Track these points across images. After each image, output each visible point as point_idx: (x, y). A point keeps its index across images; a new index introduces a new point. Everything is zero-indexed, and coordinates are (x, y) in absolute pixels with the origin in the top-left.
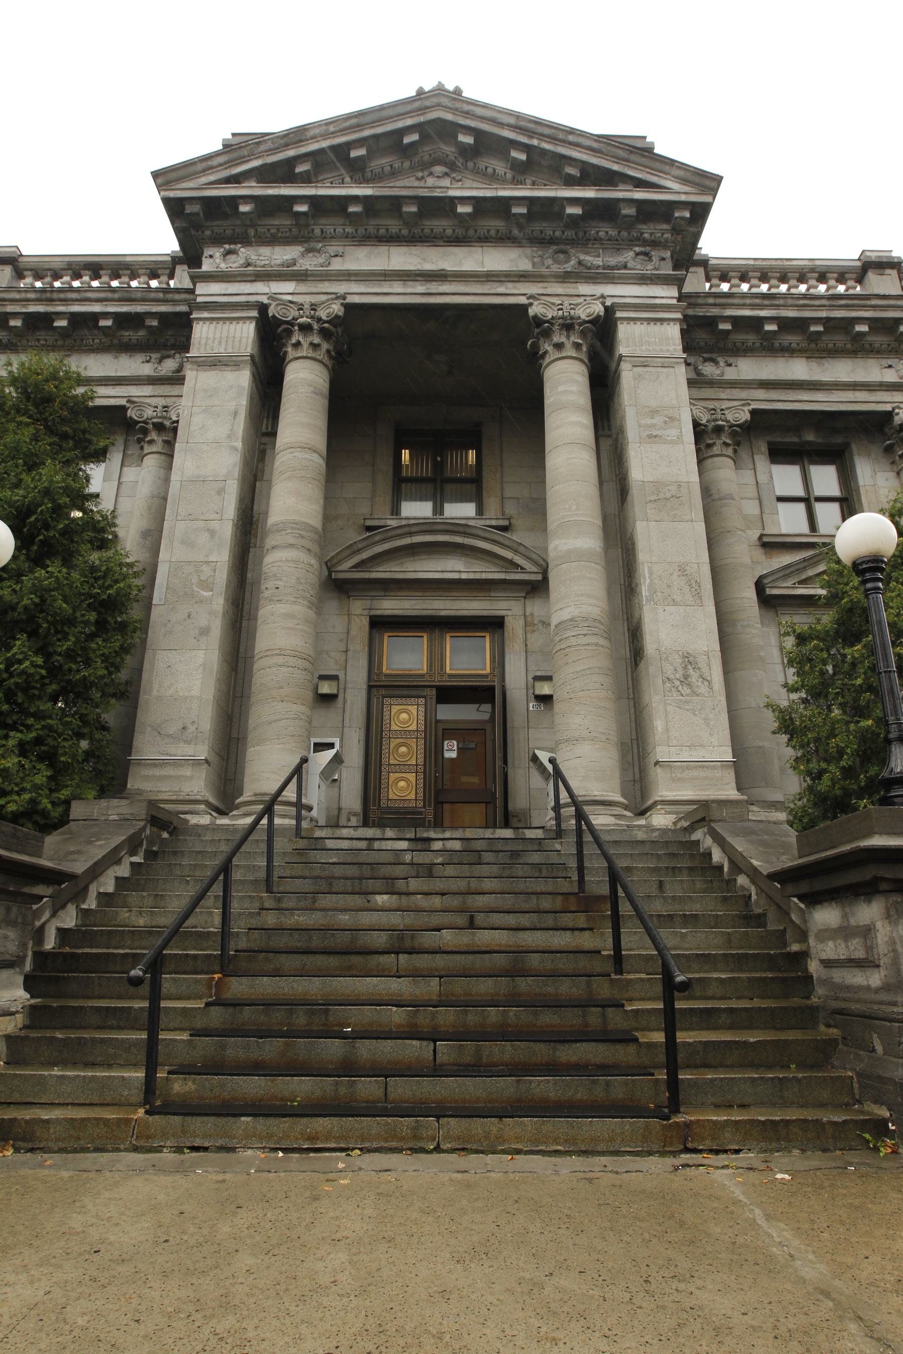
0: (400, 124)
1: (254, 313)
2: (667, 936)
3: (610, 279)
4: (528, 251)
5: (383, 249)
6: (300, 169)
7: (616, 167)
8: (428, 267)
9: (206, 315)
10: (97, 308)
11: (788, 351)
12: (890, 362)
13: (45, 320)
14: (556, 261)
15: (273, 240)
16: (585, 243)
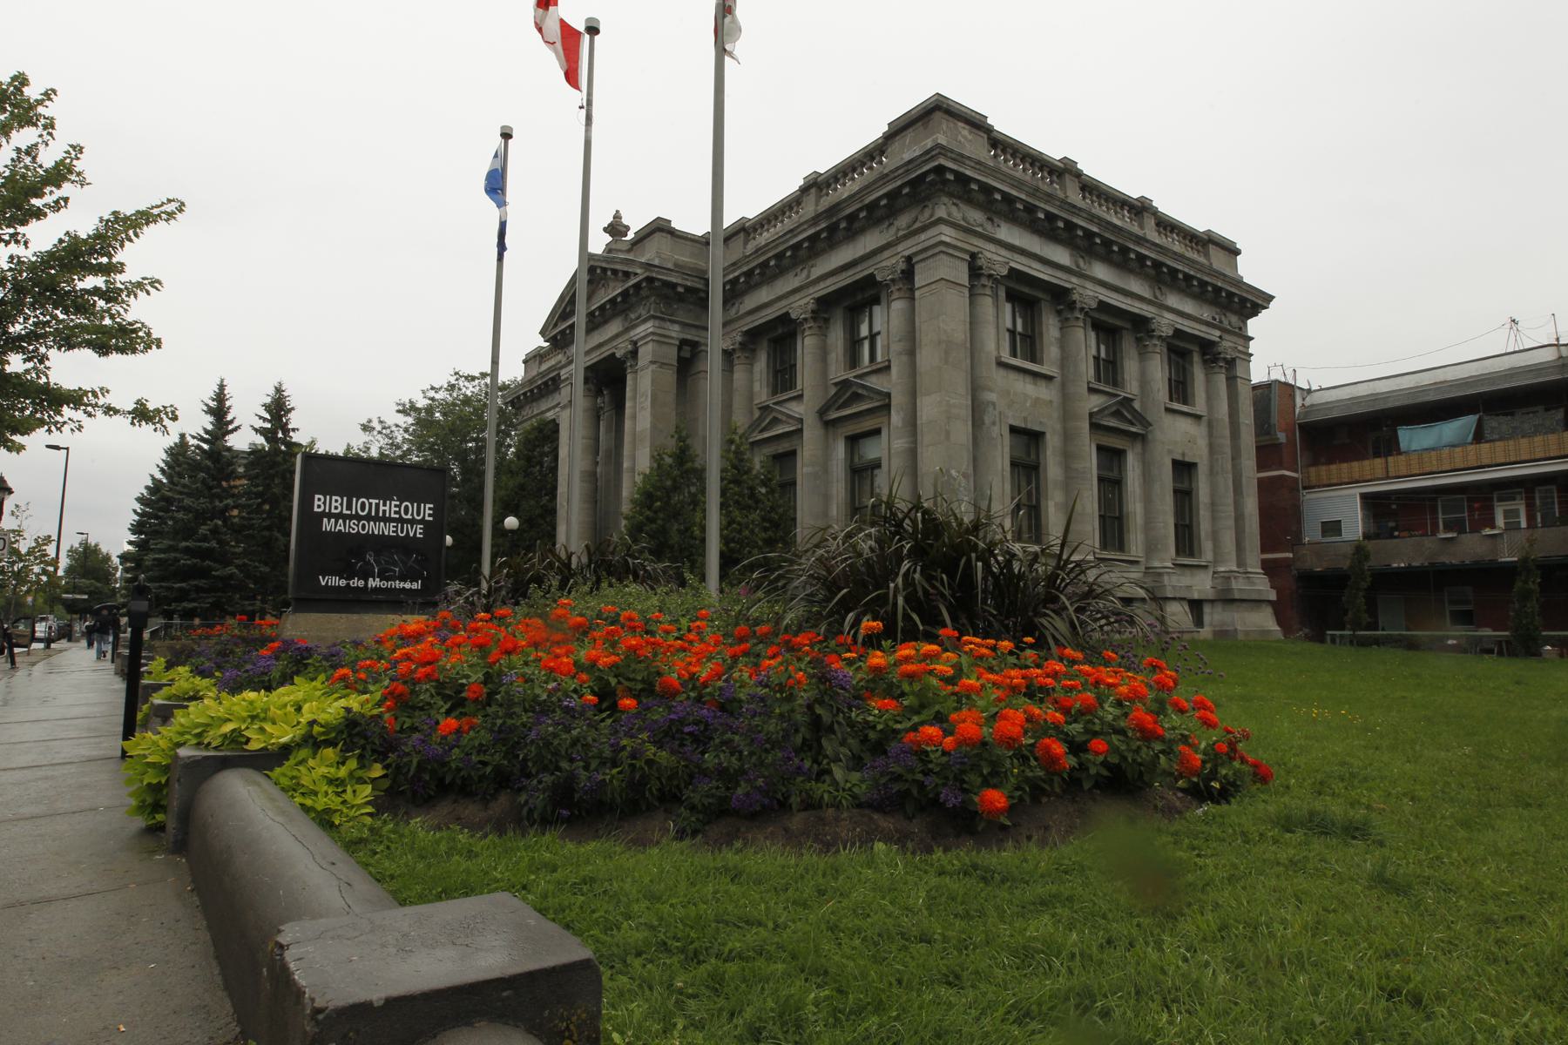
16: (630, 308)
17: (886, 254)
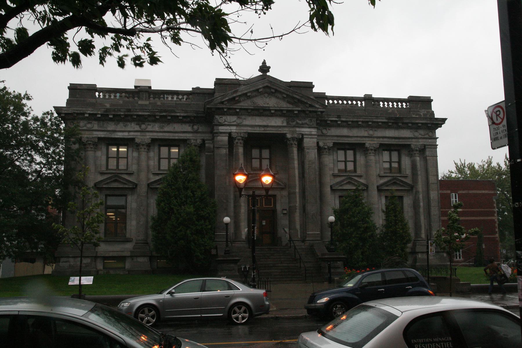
0: (258, 88)
1: (227, 135)
3: (303, 127)
4: (285, 118)
5: (255, 117)
6: (237, 99)
7: (305, 101)
8: (264, 123)
10: (178, 114)
11: (343, 127)
12: (365, 129)
13: (165, 116)
15: (231, 115)
17: (414, 140)
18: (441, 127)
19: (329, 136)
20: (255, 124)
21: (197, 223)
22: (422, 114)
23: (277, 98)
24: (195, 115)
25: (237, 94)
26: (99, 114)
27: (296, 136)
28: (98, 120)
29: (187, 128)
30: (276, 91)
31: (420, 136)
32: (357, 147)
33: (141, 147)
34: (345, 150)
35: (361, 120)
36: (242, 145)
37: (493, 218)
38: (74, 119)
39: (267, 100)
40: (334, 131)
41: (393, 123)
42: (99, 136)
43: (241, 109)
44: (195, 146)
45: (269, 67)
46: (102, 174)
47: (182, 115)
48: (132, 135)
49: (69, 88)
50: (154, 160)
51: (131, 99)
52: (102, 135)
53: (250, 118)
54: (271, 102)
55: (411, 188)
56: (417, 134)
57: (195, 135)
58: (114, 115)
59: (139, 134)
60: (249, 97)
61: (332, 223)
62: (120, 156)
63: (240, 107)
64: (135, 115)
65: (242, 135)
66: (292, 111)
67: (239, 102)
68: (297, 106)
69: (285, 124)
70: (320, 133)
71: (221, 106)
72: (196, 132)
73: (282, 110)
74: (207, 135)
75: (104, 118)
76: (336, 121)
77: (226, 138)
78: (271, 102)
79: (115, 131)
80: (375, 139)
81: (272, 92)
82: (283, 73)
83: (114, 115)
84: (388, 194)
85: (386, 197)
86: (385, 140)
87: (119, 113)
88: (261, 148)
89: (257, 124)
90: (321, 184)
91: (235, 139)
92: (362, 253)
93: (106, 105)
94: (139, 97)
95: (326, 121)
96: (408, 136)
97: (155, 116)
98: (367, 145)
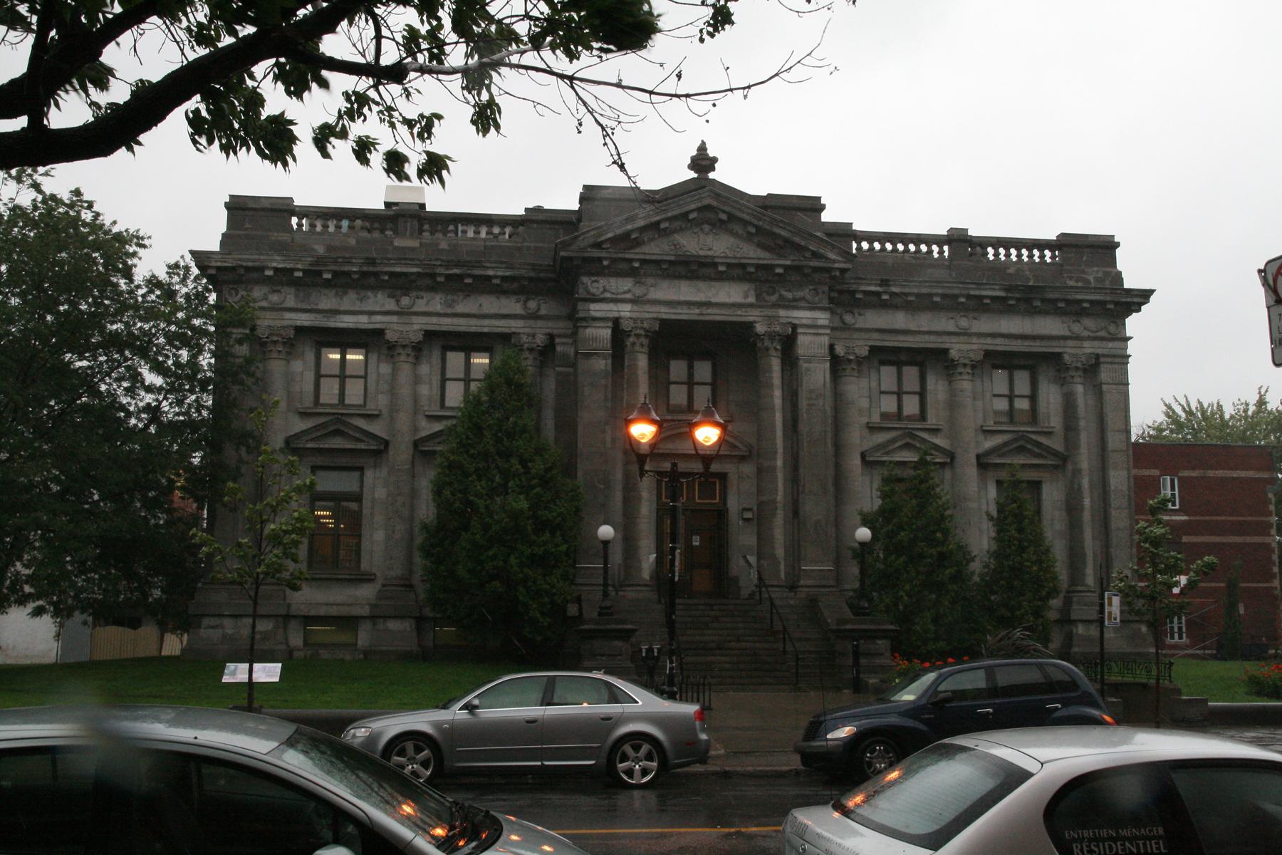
1: (610, 324)
2: (798, 645)
5: (676, 282)
7: (803, 243)
8: (700, 297)
9: (584, 324)
10: (491, 273)
13: (460, 277)
14: (768, 294)
17: (1070, 343)
18: (1139, 310)
19: (861, 330)
20: (679, 298)
21: (534, 537)
22: (1091, 278)
23: (736, 235)
24: (532, 274)
25: (636, 226)
26: (298, 270)
27: (778, 329)
28: (296, 283)
29: (512, 305)
30: (732, 217)
31: (1086, 333)
32: (931, 359)
33: (400, 351)
34: (899, 364)
35: (940, 291)
36: (645, 350)
37: (1267, 540)
38: (239, 282)
39: (709, 240)
40: (873, 319)
41: (1018, 300)
42: (299, 323)
43: (643, 262)
44: (531, 350)
45: (715, 160)
46: (304, 415)
47: (500, 273)
48: (378, 321)
49: (227, 206)
50: (430, 384)
51: (376, 235)
52: (304, 320)
53: (665, 284)
54: (720, 246)
55: (1062, 461)
56: (1077, 328)
57: (531, 322)
58: (335, 274)
59: (394, 318)
60: (665, 233)
61: (862, 544)
62: (348, 373)
63: (642, 257)
64: (386, 273)
65: (645, 325)
66: (769, 268)
67: (638, 243)
68: (780, 256)
69: (751, 300)
70: (837, 323)
71: (597, 253)
72: (534, 316)
73: (743, 266)
74: (561, 324)
75: (310, 280)
76: (878, 294)
77: (606, 333)
78: (720, 246)
79: (336, 312)
80: (974, 340)
81: (721, 221)
82: (749, 172)
83: (335, 274)
84: (1004, 475)
85: (999, 483)
86: (998, 341)
87: (346, 268)
88: (691, 358)
89: (682, 298)
90: (839, 447)
91: (628, 334)
92: (935, 620)
93: (316, 247)
94: (396, 232)
95: (853, 293)
96: (1055, 332)
97: (433, 276)
98: (953, 354)
